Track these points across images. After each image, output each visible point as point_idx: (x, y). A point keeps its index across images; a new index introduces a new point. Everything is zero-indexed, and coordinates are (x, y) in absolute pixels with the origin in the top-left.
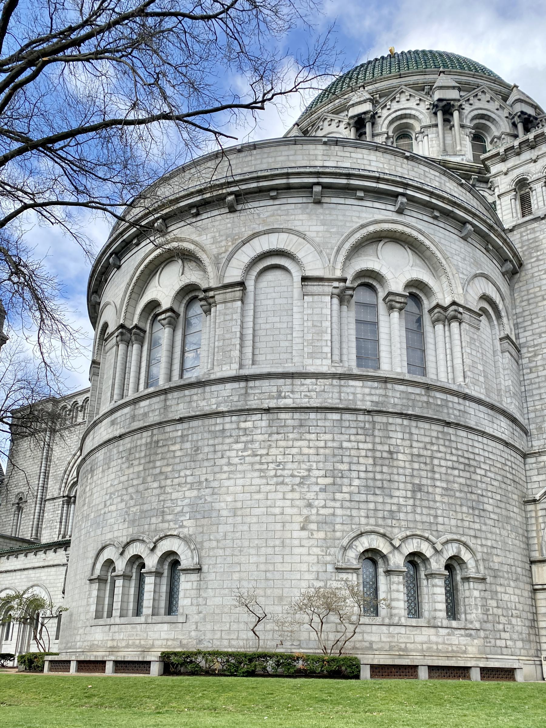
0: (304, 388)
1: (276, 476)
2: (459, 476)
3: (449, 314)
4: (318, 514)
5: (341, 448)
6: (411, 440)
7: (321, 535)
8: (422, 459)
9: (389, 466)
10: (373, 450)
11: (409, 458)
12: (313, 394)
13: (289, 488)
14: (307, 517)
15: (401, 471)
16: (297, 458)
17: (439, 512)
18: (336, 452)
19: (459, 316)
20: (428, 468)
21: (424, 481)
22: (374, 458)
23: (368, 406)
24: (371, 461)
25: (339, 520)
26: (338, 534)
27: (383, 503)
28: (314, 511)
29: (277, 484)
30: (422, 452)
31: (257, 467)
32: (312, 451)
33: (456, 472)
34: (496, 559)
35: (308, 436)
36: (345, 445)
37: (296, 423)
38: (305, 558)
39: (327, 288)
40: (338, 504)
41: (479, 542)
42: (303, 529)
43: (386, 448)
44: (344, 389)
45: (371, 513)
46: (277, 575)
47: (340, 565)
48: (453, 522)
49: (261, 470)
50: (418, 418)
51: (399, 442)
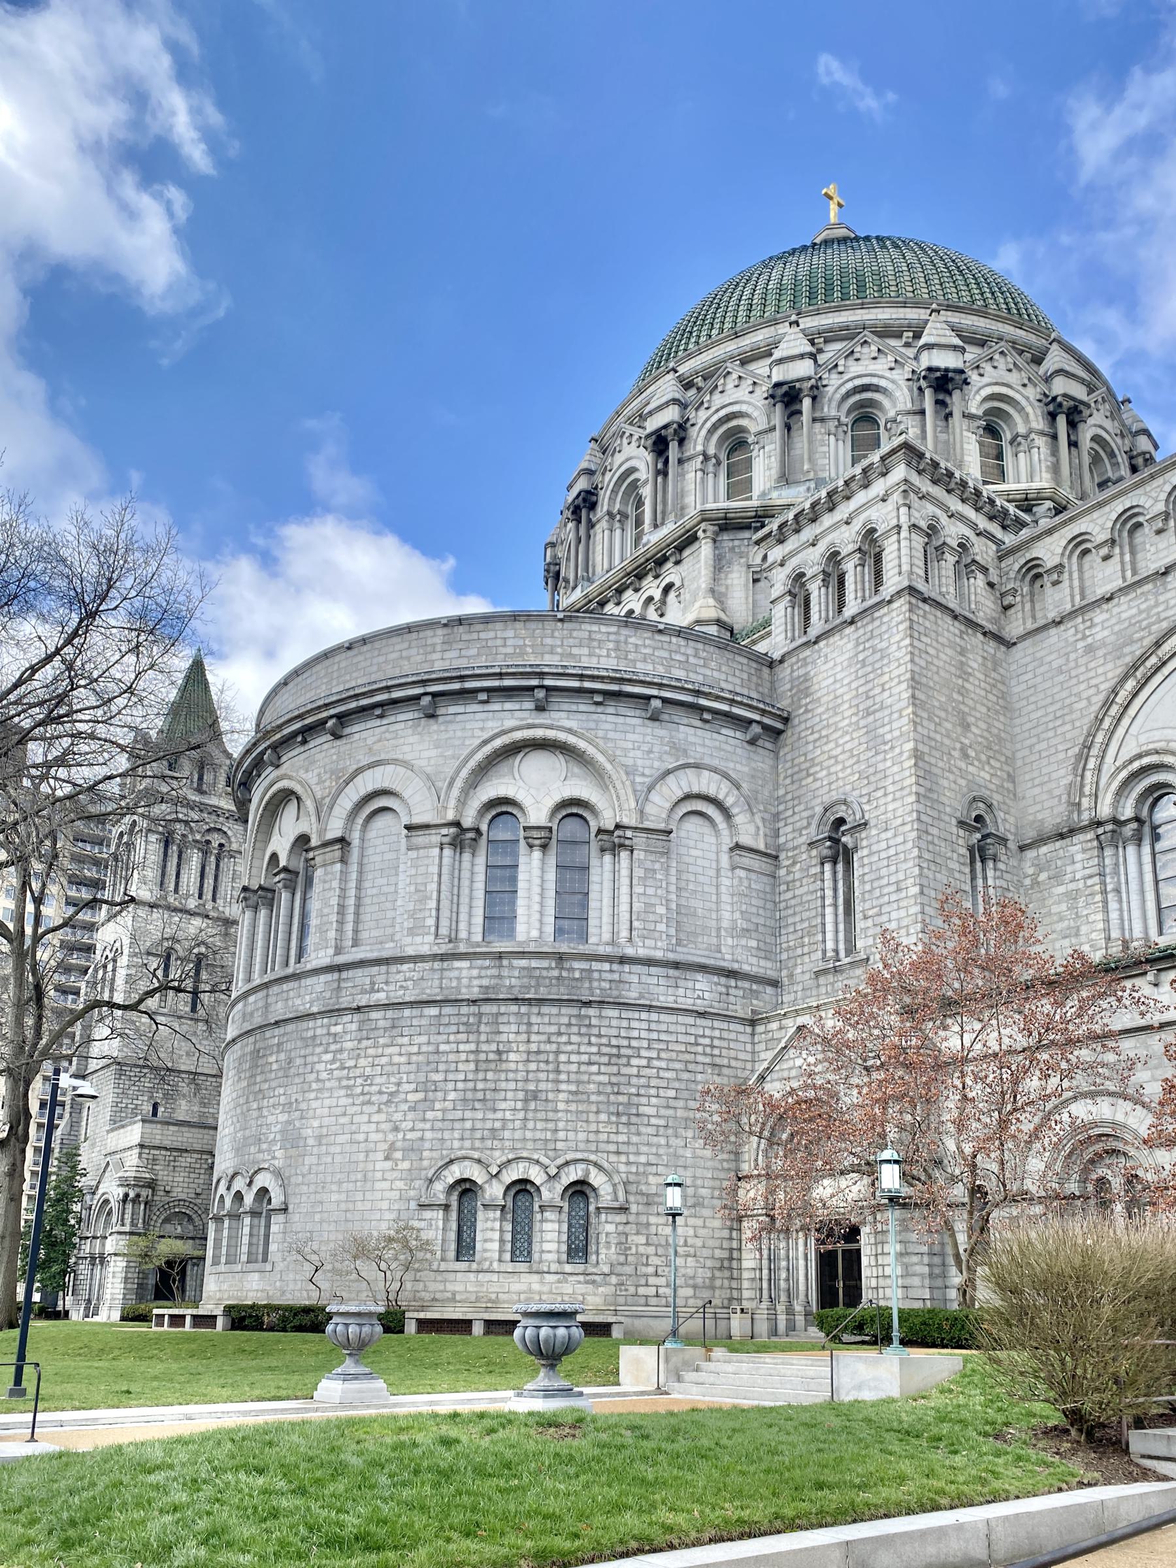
0: (400, 977)
1: (363, 1094)
2: (599, 1073)
3: (614, 841)
4: (404, 1139)
5: (437, 1052)
6: (529, 1033)
7: (406, 1165)
8: (543, 1057)
9: (495, 1071)
10: (477, 1052)
11: (525, 1057)
12: (410, 983)
13: (376, 1108)
14: (393, 1143)
15: (511, 1076)
16: (386, 1069)
17: (561, 1125)
18: (432, 1058)
19: (627, 842)
20: (551, 1067)
21: (542, 1086)
22: (477, 1062)
23: (475, 993)
24: (472, 1066)
25: (427, 1145)
26: (426, 1163)
27: (484, 1120)
28: (400, 1136)
29: (363, 1104)
30: (543, 1047)
31: (344, 1083)
32: (403, 1059)
33: (594, 1068)
34: (652, 1180)
35: (400, 1040)
36: (442, 1048)
37: (388, 1024)
38: (388, 1194)
39: (435, 838)
40: (428, 1126)
41: (623, 1158)
42: (387, 1158)
43: (494, 1047)
44: (446, 974)
45: (467, 1134)
46: (358, 1216)
47: (423, 1200)
48: (582, 1136)
49: (348, 1087)
50: (541, 1001)
51: (512, 1037)
